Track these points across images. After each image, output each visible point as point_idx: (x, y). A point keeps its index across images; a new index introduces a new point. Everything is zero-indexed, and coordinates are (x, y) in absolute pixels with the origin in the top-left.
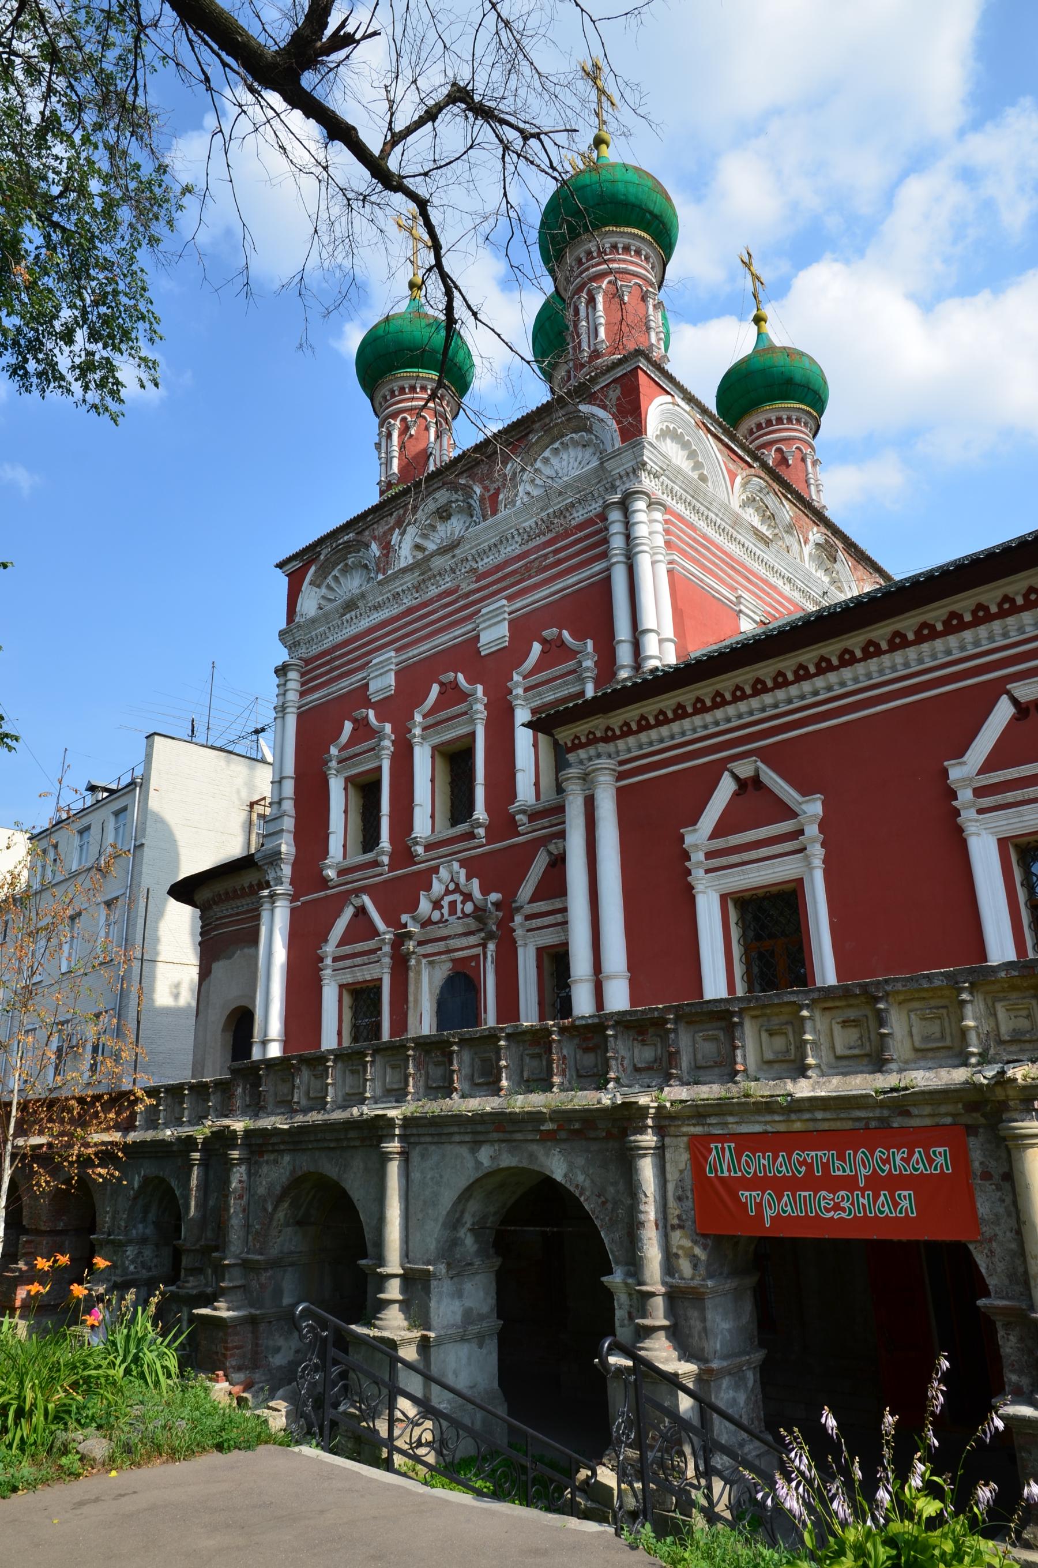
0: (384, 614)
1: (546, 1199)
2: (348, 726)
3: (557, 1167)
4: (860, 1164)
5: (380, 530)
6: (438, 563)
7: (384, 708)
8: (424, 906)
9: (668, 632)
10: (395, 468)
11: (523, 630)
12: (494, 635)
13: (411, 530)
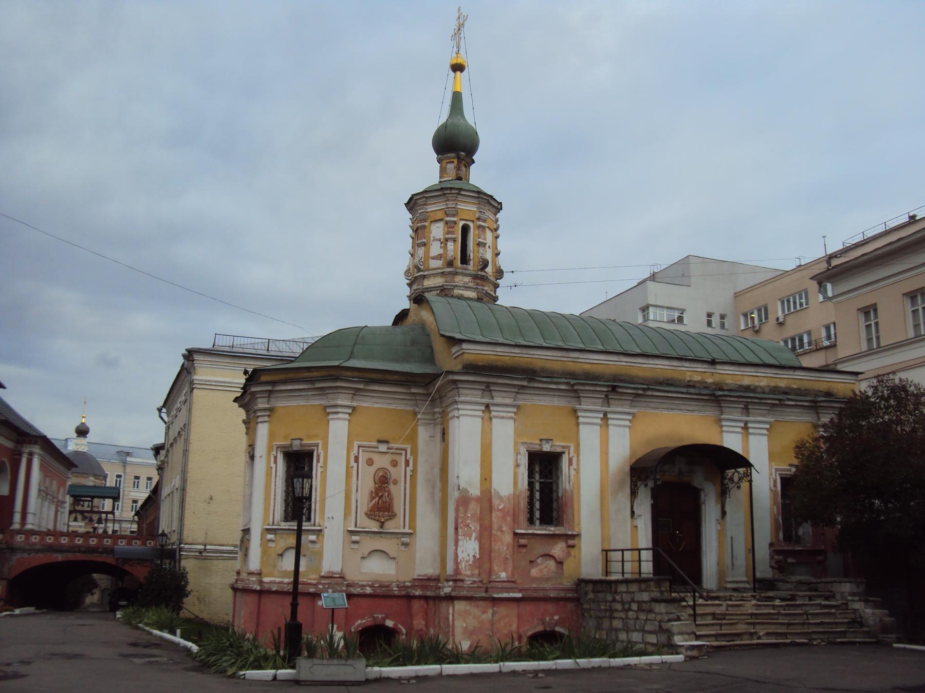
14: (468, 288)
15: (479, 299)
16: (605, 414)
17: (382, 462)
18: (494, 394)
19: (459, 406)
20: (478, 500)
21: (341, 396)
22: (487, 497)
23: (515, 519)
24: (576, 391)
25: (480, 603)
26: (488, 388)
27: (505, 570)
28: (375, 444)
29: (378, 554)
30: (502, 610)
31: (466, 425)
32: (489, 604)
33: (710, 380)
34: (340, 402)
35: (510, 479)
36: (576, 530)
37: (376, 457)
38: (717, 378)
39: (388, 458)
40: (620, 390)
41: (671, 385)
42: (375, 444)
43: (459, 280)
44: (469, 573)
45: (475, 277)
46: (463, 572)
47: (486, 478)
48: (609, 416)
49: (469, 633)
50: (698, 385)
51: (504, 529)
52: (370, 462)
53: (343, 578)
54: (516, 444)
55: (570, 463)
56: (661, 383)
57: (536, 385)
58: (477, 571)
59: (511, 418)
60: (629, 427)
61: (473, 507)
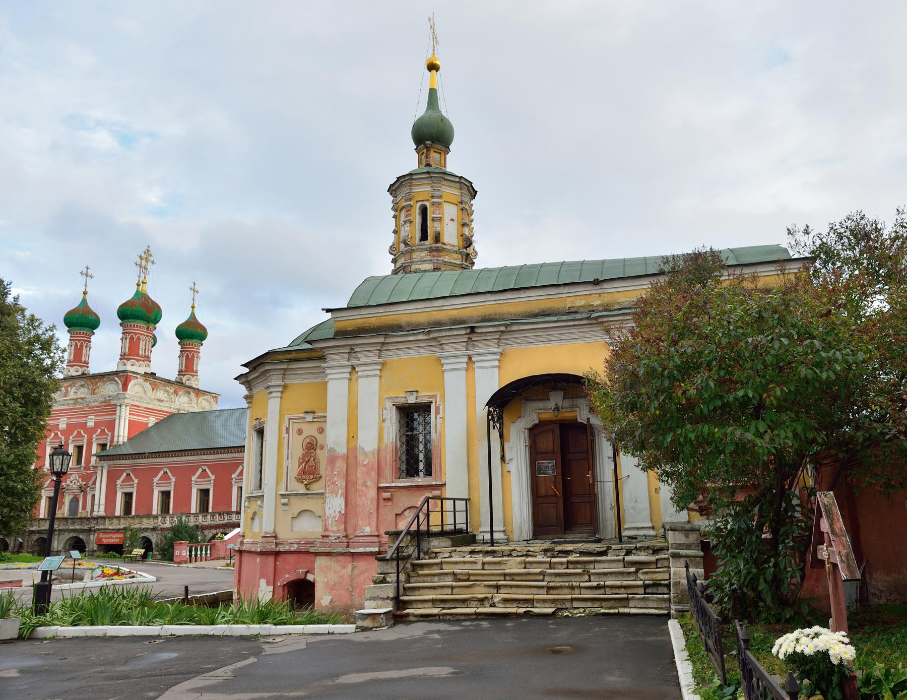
0: (65, 407)
1: (81, 540)
2: (53, 434)
3: (81, 537)
4: (115, 536)
5: (66, 384)
6: (79, 400)
7: (63, 432)
8: (68, 482)
9: (126, 434)
10: (72, 358)
11: (97, 424)
12: (91, 424)
13: (74, 388)
14: (423, 262)
15: (436, 269)
16: (470, 358)
17: (310, 430)
18: (359, 355)
19: (327, 372)
20: (347, 458)
21: (274, 377)
22: (351, 457)
23: (379, 474)
24: (435, 339)
25: (340, 558)
26: (352, 351)
27: (369, 525)
28: (303, 415)
29: (305, 513)
30: (362, 564)
31: (337, 387)
32: (349, 559)
33: (597, 302)
34: (273, 383)
35: (378, 433)
36: (443, 480)
37: (304, 427)
38: (606, 299)
39: (316, 425)
40: (480, 330)
41: (548, 315)
42: (303, 415)
43: (416, 256)
44: (335, 529)
45: (431, 250)
46: (330, 528)
47: (352, 436)
48: (474, 359)
49: (331, 588)
50: (581, 310)
51: (369, 483)
52: (300, 432)
53: (276, 537)
54: (381, 400)
55: (437, 413)
56: (536, 315)
57: (395, 340)
58: (342, 527)
59: (376, 375)
60: (499, 367)
61: (340, 465)
